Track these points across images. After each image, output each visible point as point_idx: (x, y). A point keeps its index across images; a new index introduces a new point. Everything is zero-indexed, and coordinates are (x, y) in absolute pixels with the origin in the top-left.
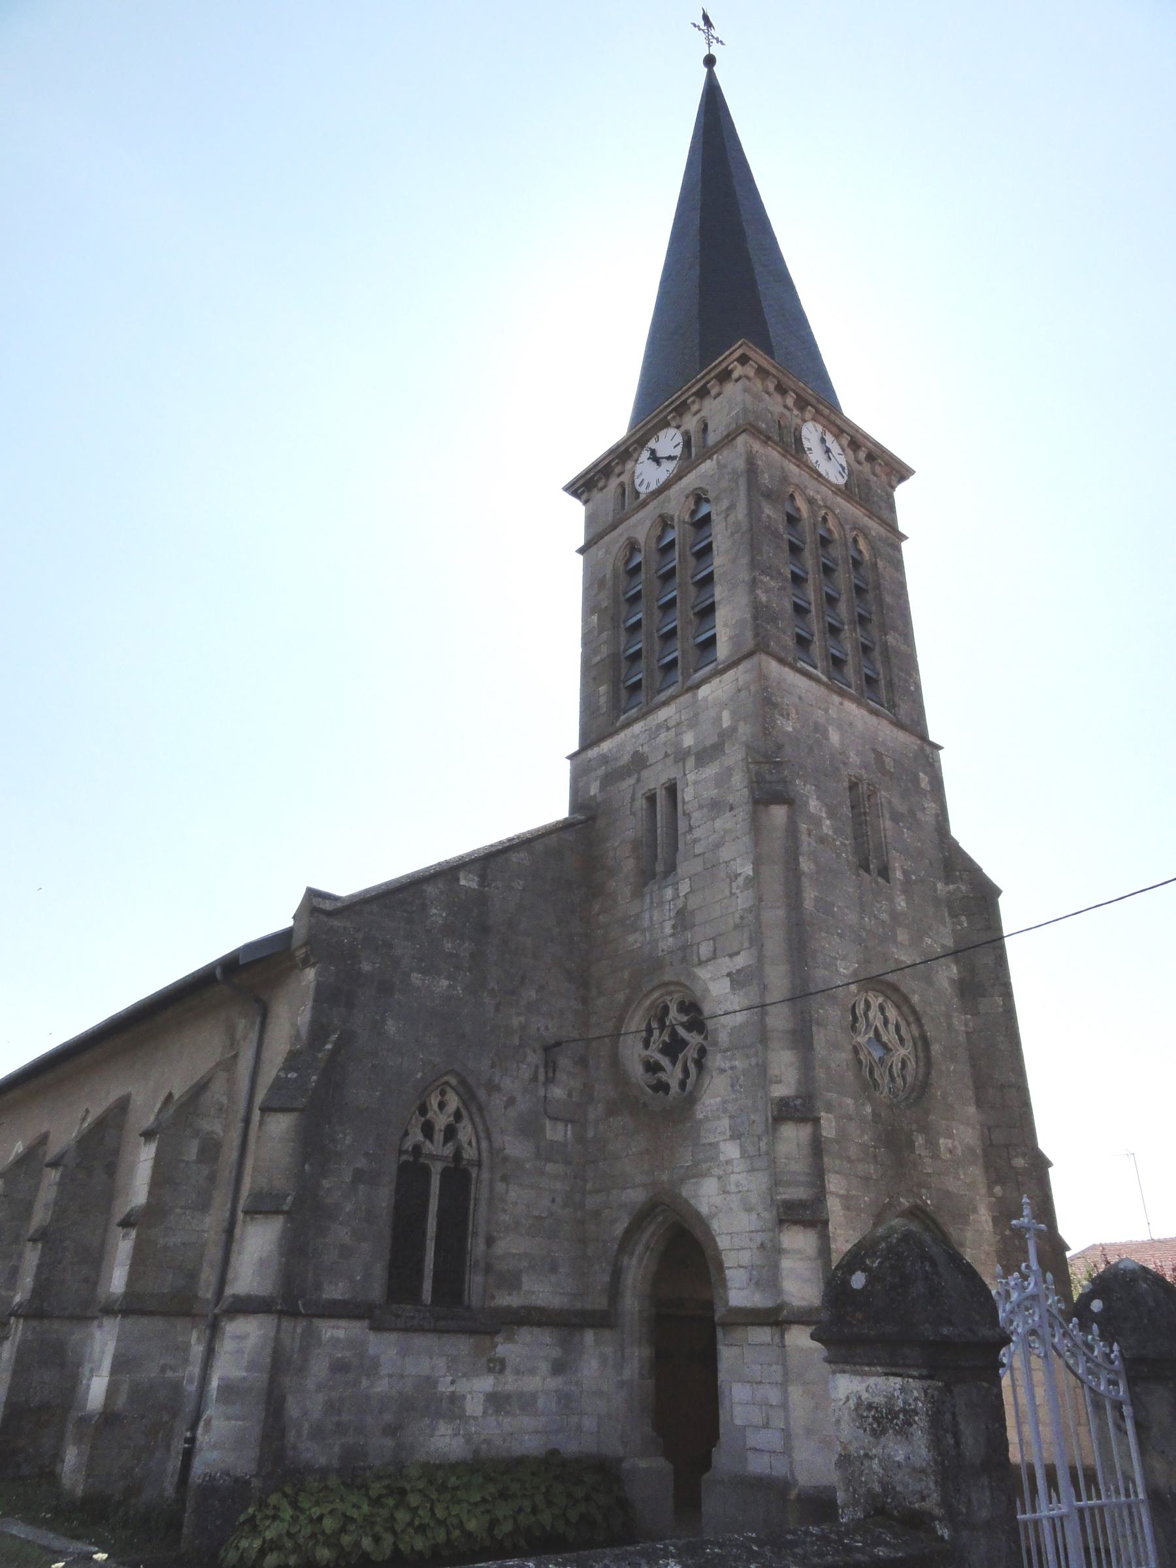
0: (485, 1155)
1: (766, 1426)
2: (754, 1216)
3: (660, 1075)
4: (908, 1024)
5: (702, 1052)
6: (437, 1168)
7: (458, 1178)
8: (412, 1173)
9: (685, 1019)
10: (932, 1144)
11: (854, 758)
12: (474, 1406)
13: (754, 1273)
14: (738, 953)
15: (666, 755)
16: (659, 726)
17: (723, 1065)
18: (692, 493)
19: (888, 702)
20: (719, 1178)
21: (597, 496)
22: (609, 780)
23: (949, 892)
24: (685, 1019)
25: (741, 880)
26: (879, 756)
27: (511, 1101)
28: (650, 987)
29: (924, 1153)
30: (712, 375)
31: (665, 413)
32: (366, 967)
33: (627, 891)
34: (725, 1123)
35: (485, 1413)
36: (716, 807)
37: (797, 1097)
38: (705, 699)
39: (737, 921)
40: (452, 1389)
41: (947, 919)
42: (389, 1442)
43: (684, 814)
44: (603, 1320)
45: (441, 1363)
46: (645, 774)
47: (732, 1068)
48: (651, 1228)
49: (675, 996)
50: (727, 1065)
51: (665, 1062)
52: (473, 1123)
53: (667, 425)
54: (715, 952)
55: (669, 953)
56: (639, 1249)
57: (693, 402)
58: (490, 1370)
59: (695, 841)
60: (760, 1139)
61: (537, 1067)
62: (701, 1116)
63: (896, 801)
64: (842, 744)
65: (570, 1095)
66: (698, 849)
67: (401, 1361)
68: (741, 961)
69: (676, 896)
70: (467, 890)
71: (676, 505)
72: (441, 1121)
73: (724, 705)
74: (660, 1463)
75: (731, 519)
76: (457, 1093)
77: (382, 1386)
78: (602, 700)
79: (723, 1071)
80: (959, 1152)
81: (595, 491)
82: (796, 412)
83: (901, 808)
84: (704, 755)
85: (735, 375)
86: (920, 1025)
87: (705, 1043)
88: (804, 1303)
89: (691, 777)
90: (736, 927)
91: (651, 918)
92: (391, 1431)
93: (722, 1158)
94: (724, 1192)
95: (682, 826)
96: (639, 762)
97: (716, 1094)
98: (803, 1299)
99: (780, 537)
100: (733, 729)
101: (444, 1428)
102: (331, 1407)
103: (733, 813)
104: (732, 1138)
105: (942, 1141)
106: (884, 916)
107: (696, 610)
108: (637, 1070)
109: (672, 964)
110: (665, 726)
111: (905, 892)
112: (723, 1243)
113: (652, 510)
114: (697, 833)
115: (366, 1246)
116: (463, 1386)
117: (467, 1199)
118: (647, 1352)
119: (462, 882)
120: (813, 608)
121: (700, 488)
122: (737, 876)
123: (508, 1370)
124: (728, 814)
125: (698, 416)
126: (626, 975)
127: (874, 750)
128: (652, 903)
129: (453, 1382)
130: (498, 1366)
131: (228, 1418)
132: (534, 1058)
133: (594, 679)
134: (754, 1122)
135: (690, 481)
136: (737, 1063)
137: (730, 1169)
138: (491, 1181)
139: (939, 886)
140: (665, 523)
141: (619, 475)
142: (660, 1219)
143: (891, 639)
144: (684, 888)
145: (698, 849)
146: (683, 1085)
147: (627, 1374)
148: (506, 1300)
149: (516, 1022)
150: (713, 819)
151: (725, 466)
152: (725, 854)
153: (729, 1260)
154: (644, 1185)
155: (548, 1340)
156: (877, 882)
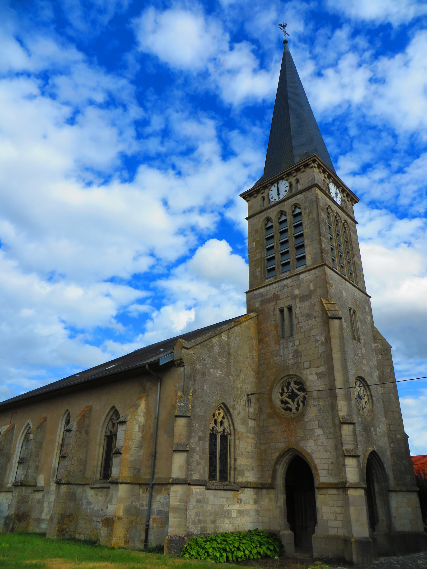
0: (232, 431)
1: (336, 520)
2: (329, 453)
3: (287, 405)
4: (366, 391)
5: (304, 398)
6: (219, 435)
7: (224, 438)
8: (213, 436)
9: (297, 387)
10: (375, 430)
11: (350, 302)
12: (234, 514)
13: (330, 471)
14: (320, 367)
15: (287, 296)
16: (284, 286)
17: (315, 404)
18: (294, 205)
19: (355, 281)
20: (315, 440)
21: (253, 200)
22: (263, 302)
23: (375, 347)
24: (297, 387)
25: (320, 342)
26: (356, 300)
27: (239, 413)
28: (284, 375)
29: (374, 433)
30: (302, 164)
31: (282, 175)
32: (198, 367)
33: (273, 342)
34: (317, 422)
35: (237, 516)
36: (309, 316)
37: (347, 416)
38: (303, 279)
39: (319, 356)
40: (228, 509)
41: (375, 356)
42: (213, 526)
43: (296, 317)
44: (270, 487)
45: (224, 500)
46: (279, 302)
47: (319, 405)
48: (287, 456)
49: (293, 379)
50: (316, 404)
51: (290, 401)
52: (228, 419)
53: (282, 178)
54: (310, 366)
55: (291, 364)
56: (283, 463)
57: (294, 173)
58: (238, 502)
59: (300, 327)
60: (330, 429)
61: (246, 401)
62: (307, 420)
63: (360, 316)
64: (346, 296)
65: (255, 411)
66: (302, 330)
67: (217, 499)
68: (321, 369)
69: (294, 345)
70: (224, 340)
71: (287, 207)
72: (220, 419)
73: (311, 281)
74: (290, 532)
75: (311, 216)
76: (223, 410)
77: (210, 508)
78: (259, 274)
79: (315, 406)
80: (382, 433)
81: (252, 198)
82: (327, 179)
83: (362, 318)
84: (304, 298)
85: (311, 166)
86: (370, 391)
87: (306, 396)
88: (353, 482)
89: (298, 305)
90: (318, 358)
91: (284, 352)
92: (213, 522)
93: (316, 434)
94: (317, 445)
95: (295, 322)
96: (276, 298)
97: (312, 413)
98: (353, 480)
99: (326, 224)
100: (315, 290)
101: (227, 521)
102: (197, 514)
103: (316, 319)
104: (319, 428)
105: (378, 429)
106: (360, 355)
107: (296, 246)
108: (278, 403)
109: (293, 368)
110: (287, 286)
111: (364, 347)
112: (317, 462)
113: (276, 209)
114: (301, 325)
115: (203, 462)
116: (231, 508)
117: (227, 445)
118: (285, 496)
119: (223, 338)
120: (335, 249)
121: (298, 204)
122: (318, 341)
123: (242, 503)
124: (314, 319)
125: (295, 178)
126: (274, 371)
127: (354, 298)
128: (284, 347)
129: (228, 506)
130: (239, 501)
131: (175, 518)
132: (245, 398)
133: (255, 265)
134: (328, 423)
135: (293, 201)
136: (320, 403)
137: (318, 437)
138: (235, 440)
139: (373, 344)
140: (282, 213)
141: (262, 193)
142: (291, 453)
143: (356, 259)
144: (297, 343)
145: (302, 330)
146: (297, 409)
147: (279, 504)
148: (240, 479)
149: (239, 386)
150: (308, 321)
151: (307, 197)
152: (313, 333)
153: (319, 467)
154: (284, 442)
155: (252, 493)
156: (353, 342)
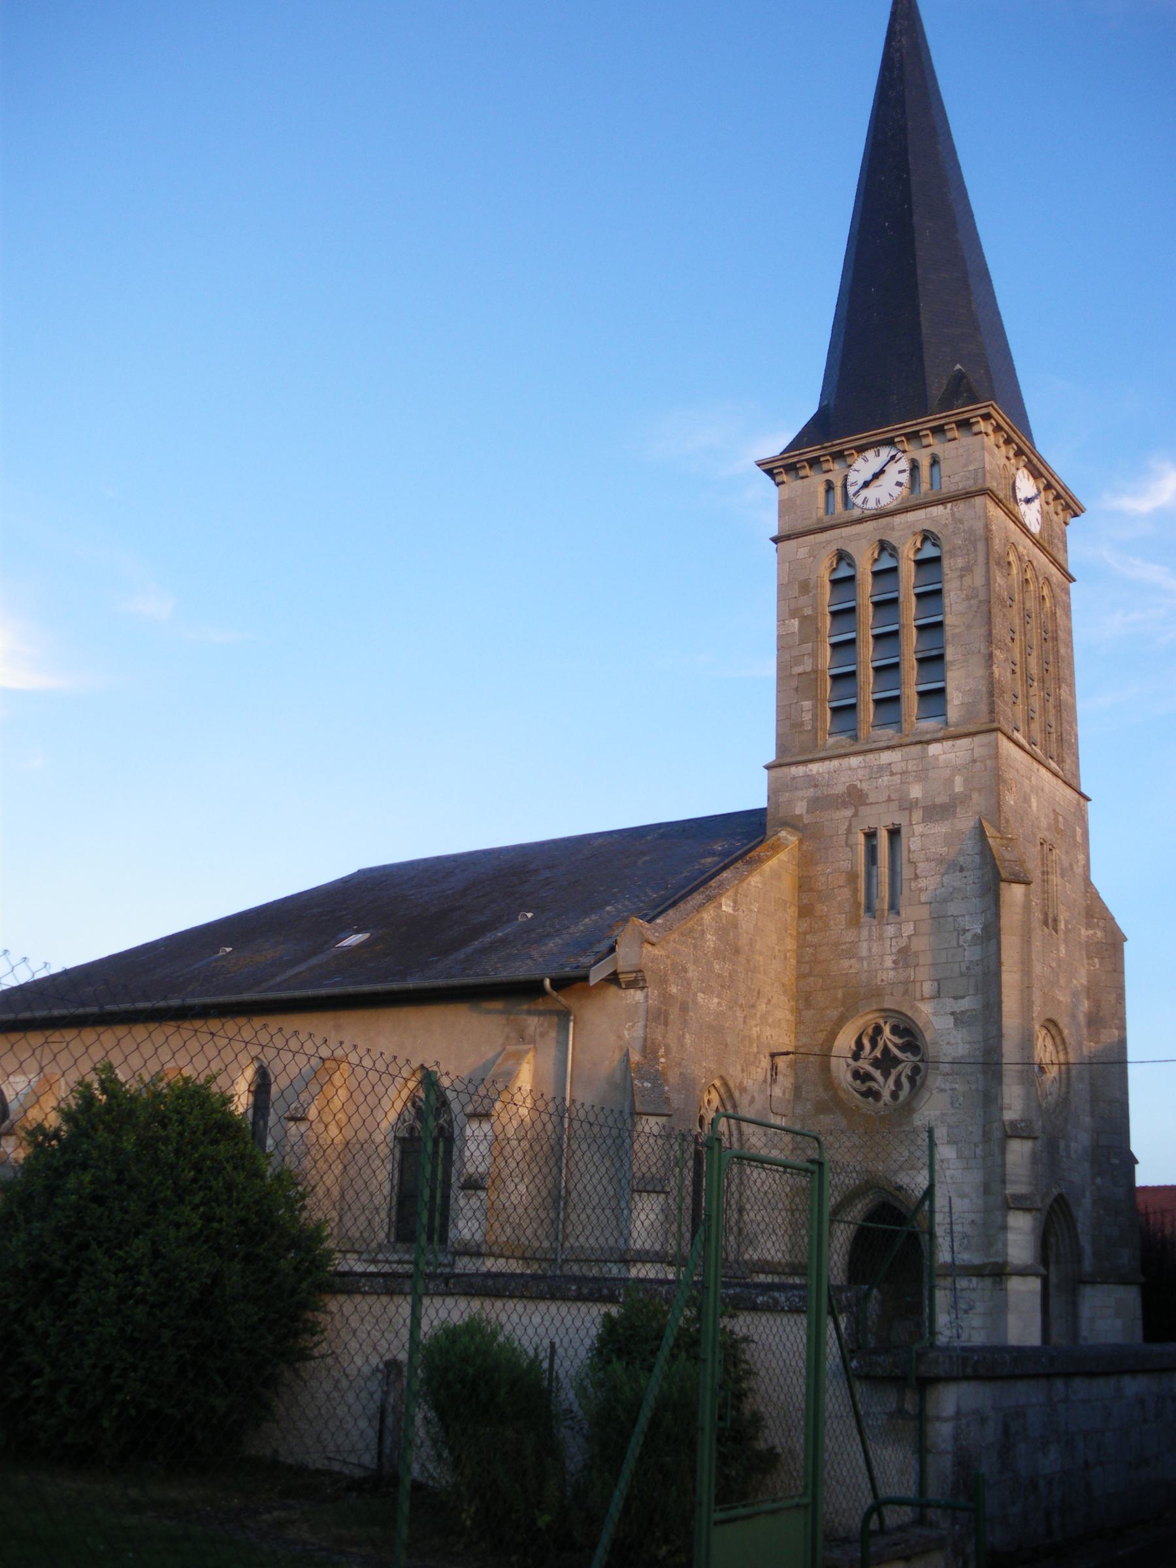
14: (963, 997)
15: (889, 800)
16: (881, 768)
17: (943, 1086)
22: (816, 804)
24: (899, 1041)
25: (969, 936)
27: (752, 1101)
32: (674, 990)
37: (1022, 1121)
38: (936, 757)
39: (964, 969)
43: (910, 862)
46: (863, 810)
47: (953, 1089)
50: (948, 1086)
51: (877, 1074)
54: (939, 991)
59: (921, 890)
60: (976, 1146)
65: (784, 1094)
68: (965, 1004)
73: (956, 770)
75: (967, 580)
79: (942, 1090)
84: (935, 812)
87: (920, 1064)
89: (919, 829)
90: (962, 975)
91: (870, 950)
95: (906, 872)
96: (855, 797)
100: (965, 798)
103: (964, 874)
104: (948, 1143)
106: (1054, 964)
109: (892, 994)
111: (1065, 941)
119: (724, 908)
121: (932, 533)
122: (965, 931)
124: (958, 874)
126: (840, 994)
127: (1054, 811)
132: (765, 1062)
133: (797, 689)
136: (957, 1086)
139: (1083, 931)
144: (908, 929)
146: (895, 1095)
